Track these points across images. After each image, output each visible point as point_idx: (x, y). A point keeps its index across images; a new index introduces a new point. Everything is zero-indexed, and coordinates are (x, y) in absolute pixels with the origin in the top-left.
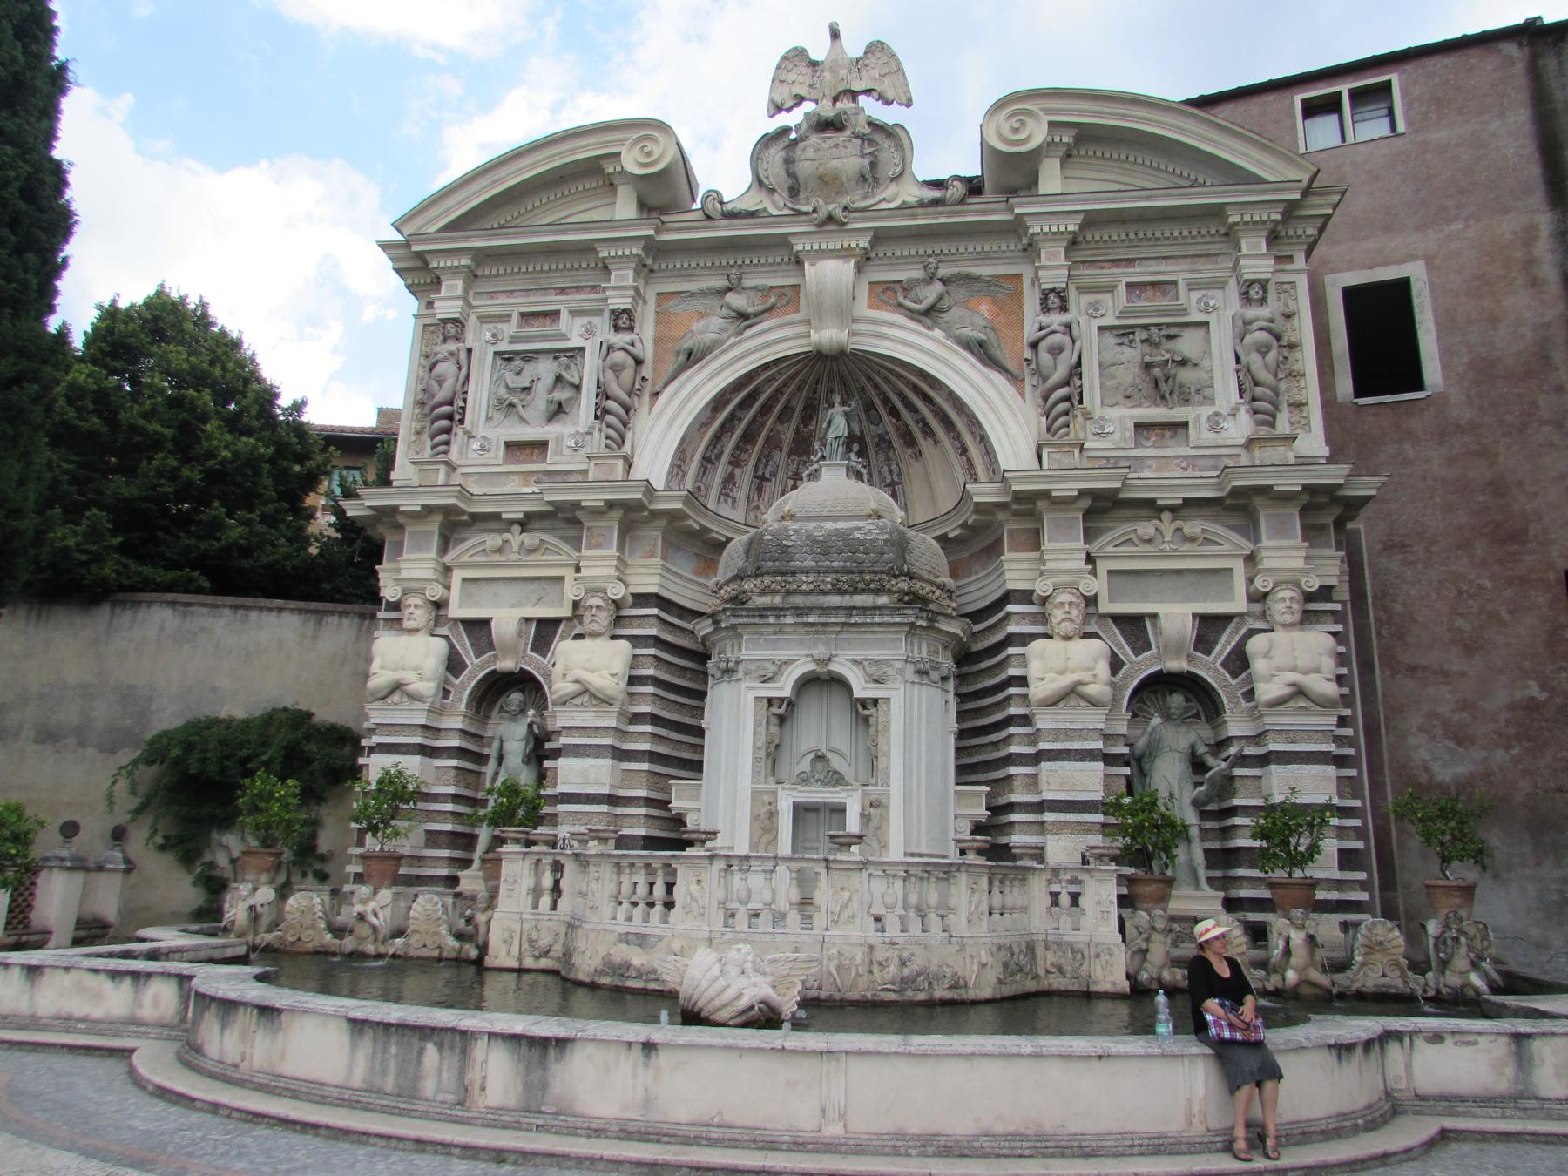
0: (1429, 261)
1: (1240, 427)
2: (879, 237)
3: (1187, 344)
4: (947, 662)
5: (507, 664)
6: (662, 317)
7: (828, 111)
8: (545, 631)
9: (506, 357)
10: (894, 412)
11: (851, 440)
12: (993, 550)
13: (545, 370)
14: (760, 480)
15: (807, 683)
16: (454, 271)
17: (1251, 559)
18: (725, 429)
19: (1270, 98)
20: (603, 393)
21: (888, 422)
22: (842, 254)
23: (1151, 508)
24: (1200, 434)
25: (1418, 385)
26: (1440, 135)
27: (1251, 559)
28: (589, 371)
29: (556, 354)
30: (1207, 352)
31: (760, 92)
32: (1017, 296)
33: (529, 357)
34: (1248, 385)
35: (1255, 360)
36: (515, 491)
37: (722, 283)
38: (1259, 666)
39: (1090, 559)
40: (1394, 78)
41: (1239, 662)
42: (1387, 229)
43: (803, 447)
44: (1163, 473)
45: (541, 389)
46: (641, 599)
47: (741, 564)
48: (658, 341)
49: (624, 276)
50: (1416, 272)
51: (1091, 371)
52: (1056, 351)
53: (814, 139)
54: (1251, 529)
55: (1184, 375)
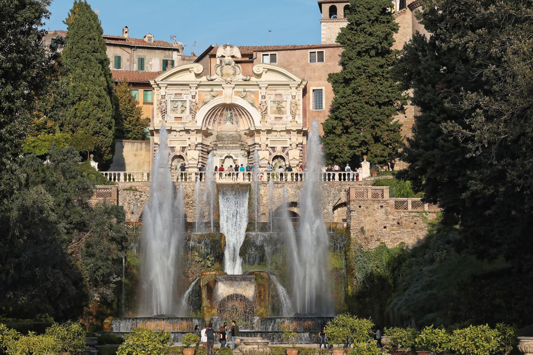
0: (325, 86)
1: (290, 118)
2: (236, 85)
3: (283, 104)
4: (246, 153)
5: (178, 154)
6: (199, 95)
9: (172, 101)
13: (180, 104)
15: (226, 157)
19: (304, 50)
20: (191, 109)
21: (237, 112)
23: (276, 131)
24: (284, 119)
25: (322, 109)
26: (329, 63)
27: (290, 139)
28: (188, 105)
29: (182, 101)
30: (286, 106)
32: (258, 94)
33: (177, 101)
34: (292, 112)
35: (293, 109)
36: (178, 126)
37: (210, 90)
39: (267, 139)
41: (287, 154)
42: (320, 80)
43: (221, 115)
44: (278, 127)
45: (179, 107)
46: (199, 144)
47: (216, 139)
48: (199, 99)
49: (193, 91)
50: (323, 88)
51: (269, 109)
52: (263, 106)
53: (225, 66)
55: (283, 109)
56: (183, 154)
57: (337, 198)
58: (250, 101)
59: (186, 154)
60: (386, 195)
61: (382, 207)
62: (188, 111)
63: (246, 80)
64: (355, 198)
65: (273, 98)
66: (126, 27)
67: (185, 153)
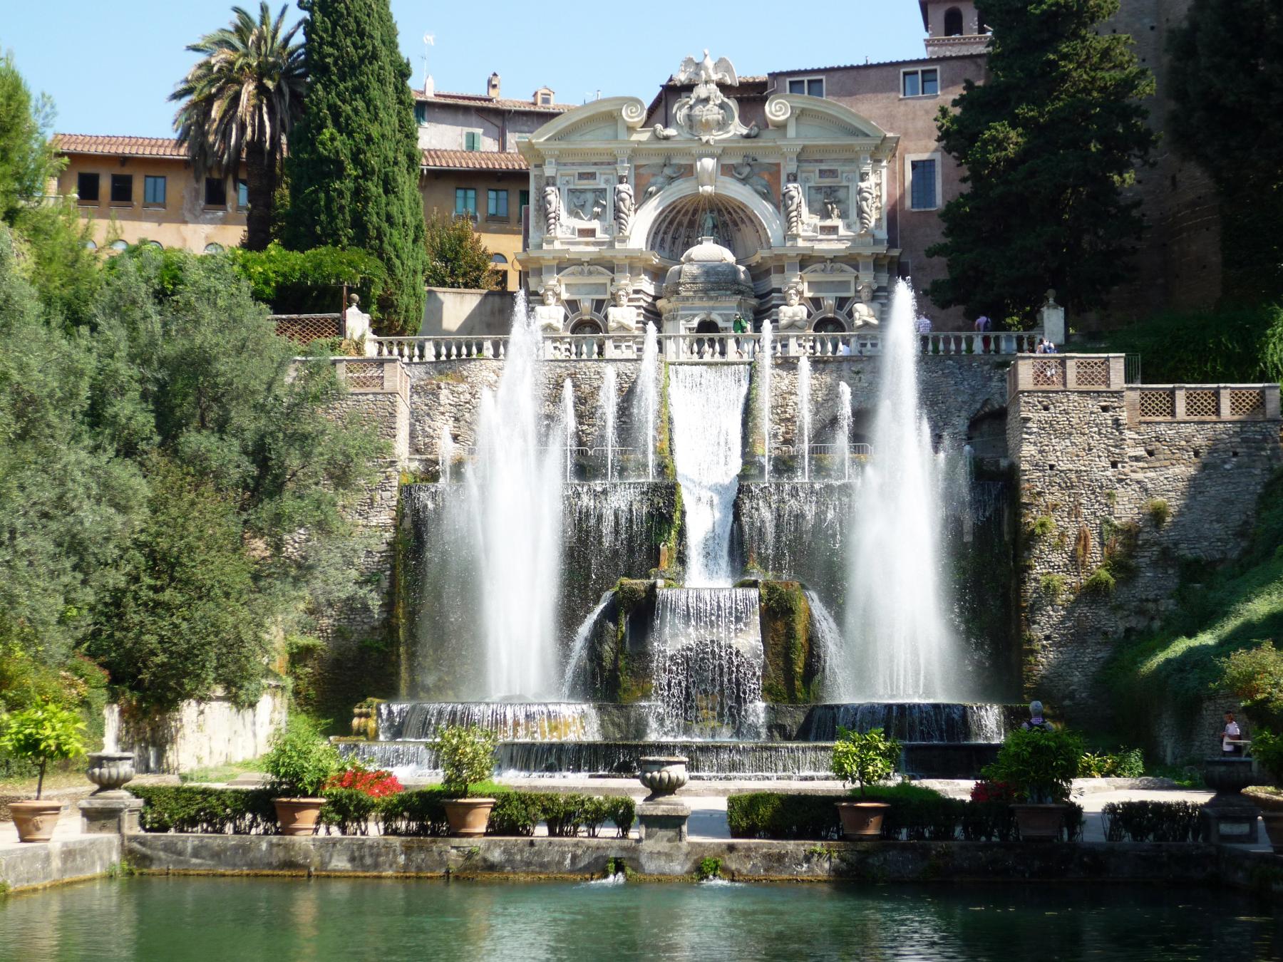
5: (587, 318)
8: (599, 305)
10: (729, 213)
11: (715, 226)
12: (767, 272)
13: (590, 197)
14: (674, 239)
16: (552, 156)
17: (857, 277)
18: (664, 220)
21: (727, 217)
22: (711, 156)
27: (857, 277)
29: (595, 191)
32: (779, 171)
33: (583, 191)
38: (857, 315)
40: (938, 67)
41: (850, 314)
43: (691, 224)
54: (856, 268)
56: (598, 318)
57: (980, 398)
58: (759, 188)
59: (606, 317)
60: (1117, 378)
61: (1105, 409)
62: (610, 213)
63: (748, 137)
64: (1031, 387)
65: (816, 180)
66: (495, 75)
67: (602, 315)
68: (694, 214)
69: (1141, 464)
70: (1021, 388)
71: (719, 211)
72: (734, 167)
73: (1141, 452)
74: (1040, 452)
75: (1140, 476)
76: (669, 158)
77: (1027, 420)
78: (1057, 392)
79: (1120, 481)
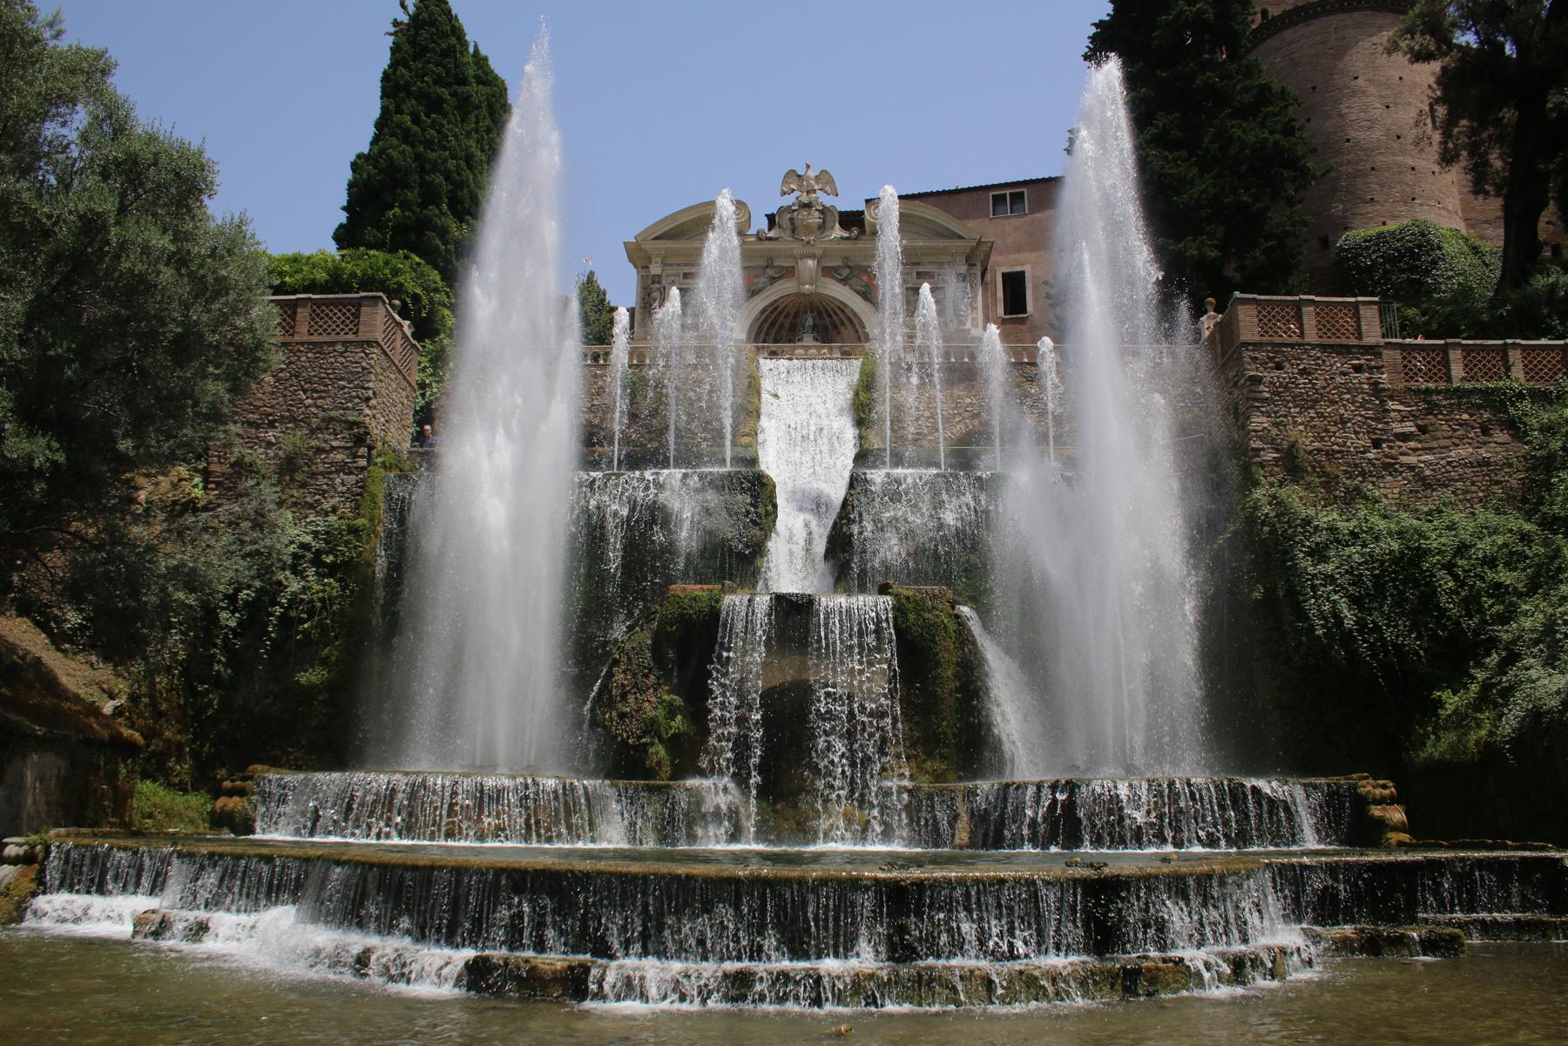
7: (805, 199)
11: (814, 327)
18: (765, 321)
21: (827, 320)
22: (812, 257)
25: (1025, 311)
31: (778, 187)
50: (1027, 268)
61: (1358, 369)
64: (1257, 338)
68: (795, 317)
69: (1412, 444)
70: (1243, 338)
71: (820, 313)
72: (835, 269)
73: (1409, 427)
74: (1276, 424)
75: (1412, 459)
76: (771, 259)
77: (1257, 380)
78: (1292, 346)
79: (1386, 466)
